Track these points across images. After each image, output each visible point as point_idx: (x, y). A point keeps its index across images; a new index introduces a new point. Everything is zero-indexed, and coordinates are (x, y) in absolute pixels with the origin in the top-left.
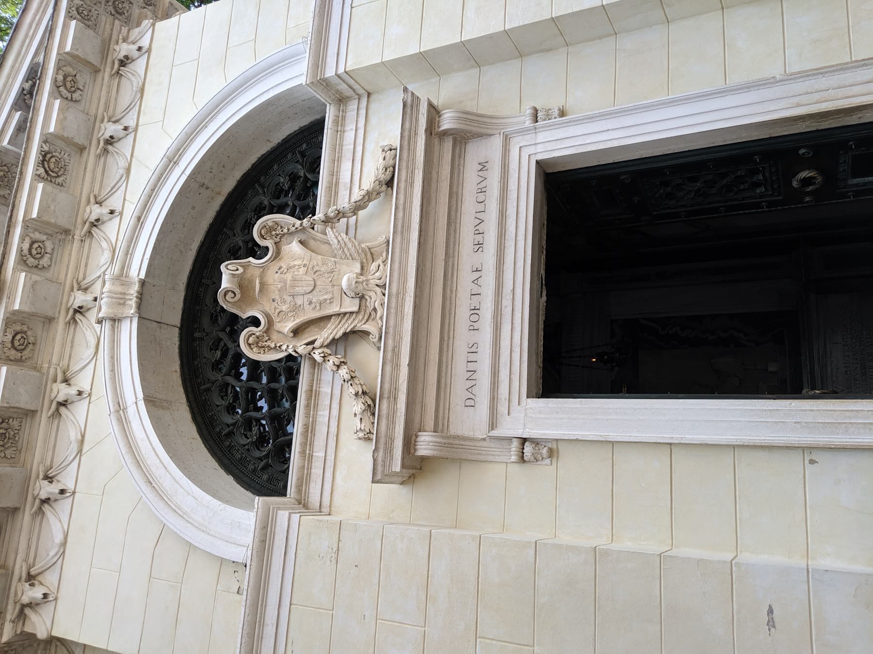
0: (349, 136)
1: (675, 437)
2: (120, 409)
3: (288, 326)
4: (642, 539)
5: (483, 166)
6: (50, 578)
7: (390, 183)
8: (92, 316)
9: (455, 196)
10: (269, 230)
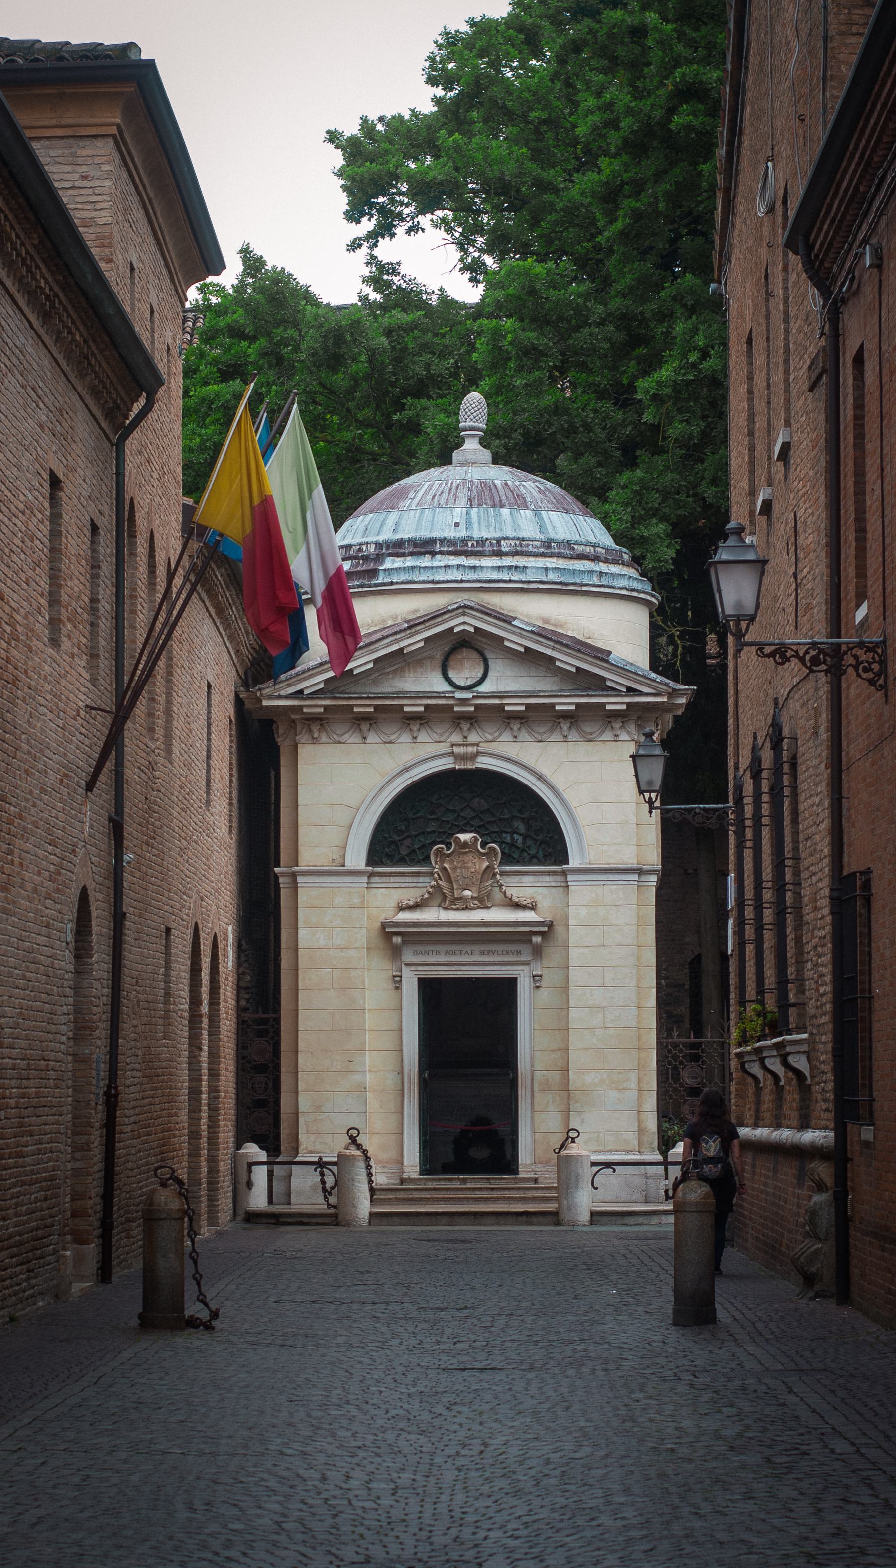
0: (547, 878)
1: (404, 1033)
2: (407, 769)
3: (447, 865)
4: (369, 1021)
5: (519, 953)
6: (324, 738)
7: (517, 906)
8: (456, 738)
9: (505, 941)
10: (494, 849)
